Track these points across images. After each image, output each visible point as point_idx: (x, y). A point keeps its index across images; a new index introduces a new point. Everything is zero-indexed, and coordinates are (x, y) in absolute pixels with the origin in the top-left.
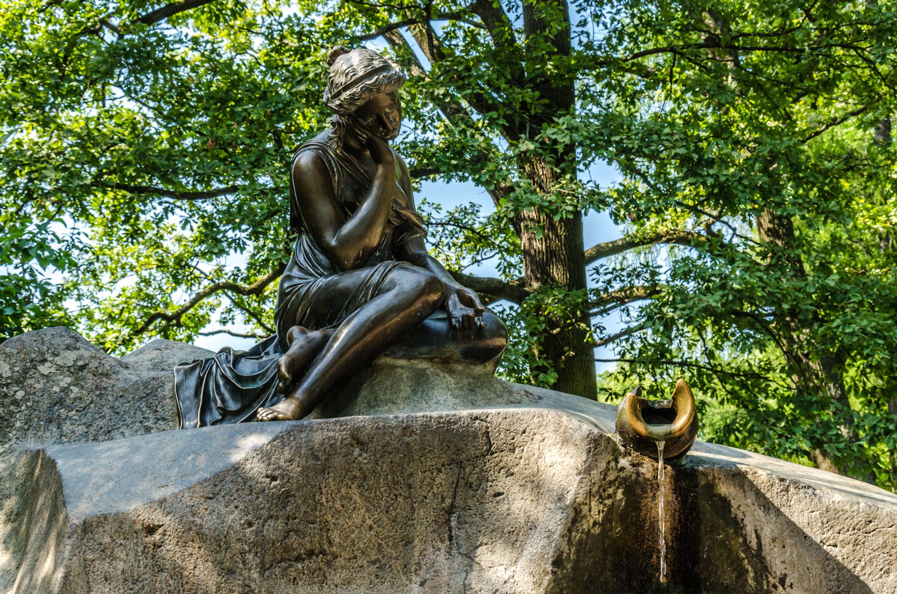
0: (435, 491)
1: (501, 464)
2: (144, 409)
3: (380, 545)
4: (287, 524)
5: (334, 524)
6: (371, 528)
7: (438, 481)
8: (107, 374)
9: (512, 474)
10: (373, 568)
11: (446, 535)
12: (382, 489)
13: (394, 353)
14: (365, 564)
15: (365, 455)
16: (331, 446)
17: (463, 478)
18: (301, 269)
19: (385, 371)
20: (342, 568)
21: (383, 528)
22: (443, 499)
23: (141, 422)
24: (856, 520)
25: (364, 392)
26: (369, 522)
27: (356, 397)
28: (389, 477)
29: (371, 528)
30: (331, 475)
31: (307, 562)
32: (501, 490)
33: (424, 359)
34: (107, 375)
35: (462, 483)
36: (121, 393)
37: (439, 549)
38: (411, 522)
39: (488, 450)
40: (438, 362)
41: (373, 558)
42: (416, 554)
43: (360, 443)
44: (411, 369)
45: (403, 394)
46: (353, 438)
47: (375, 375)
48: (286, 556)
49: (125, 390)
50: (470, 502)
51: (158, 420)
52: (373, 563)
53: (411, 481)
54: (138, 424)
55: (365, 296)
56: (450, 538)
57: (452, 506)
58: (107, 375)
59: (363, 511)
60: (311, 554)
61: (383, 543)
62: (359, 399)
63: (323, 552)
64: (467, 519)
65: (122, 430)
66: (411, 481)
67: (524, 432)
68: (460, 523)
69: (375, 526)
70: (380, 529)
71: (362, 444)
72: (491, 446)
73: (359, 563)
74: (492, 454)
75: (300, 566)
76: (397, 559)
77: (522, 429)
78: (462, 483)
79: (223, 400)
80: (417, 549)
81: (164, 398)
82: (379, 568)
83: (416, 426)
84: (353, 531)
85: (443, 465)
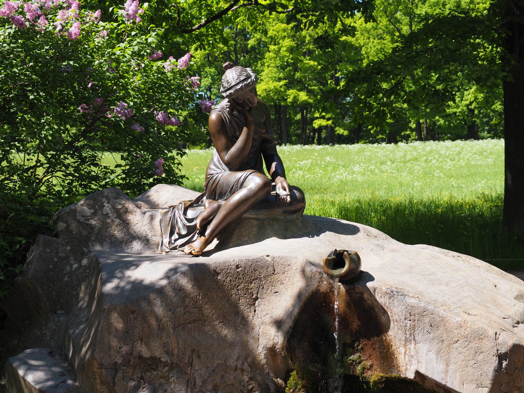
1: (279, 279)
4: (185, 309)
6: (221, 309)
8: (131, 212)
18: (215, 165)
20: (208, 326)
24: (419, 311)
26: (220, 306)
30: (204, 288)
31: (193, 324)
32: (278, 291)
44: (258, 219)
48: (184, 322)
60: (195, 321)
63: (200, 320)
67: (289, 265)
72: (274, 271)
74: (275, 275)
75: (190, 325)
77: (288, 264)
79: (179, 229)
83: (242, 264)
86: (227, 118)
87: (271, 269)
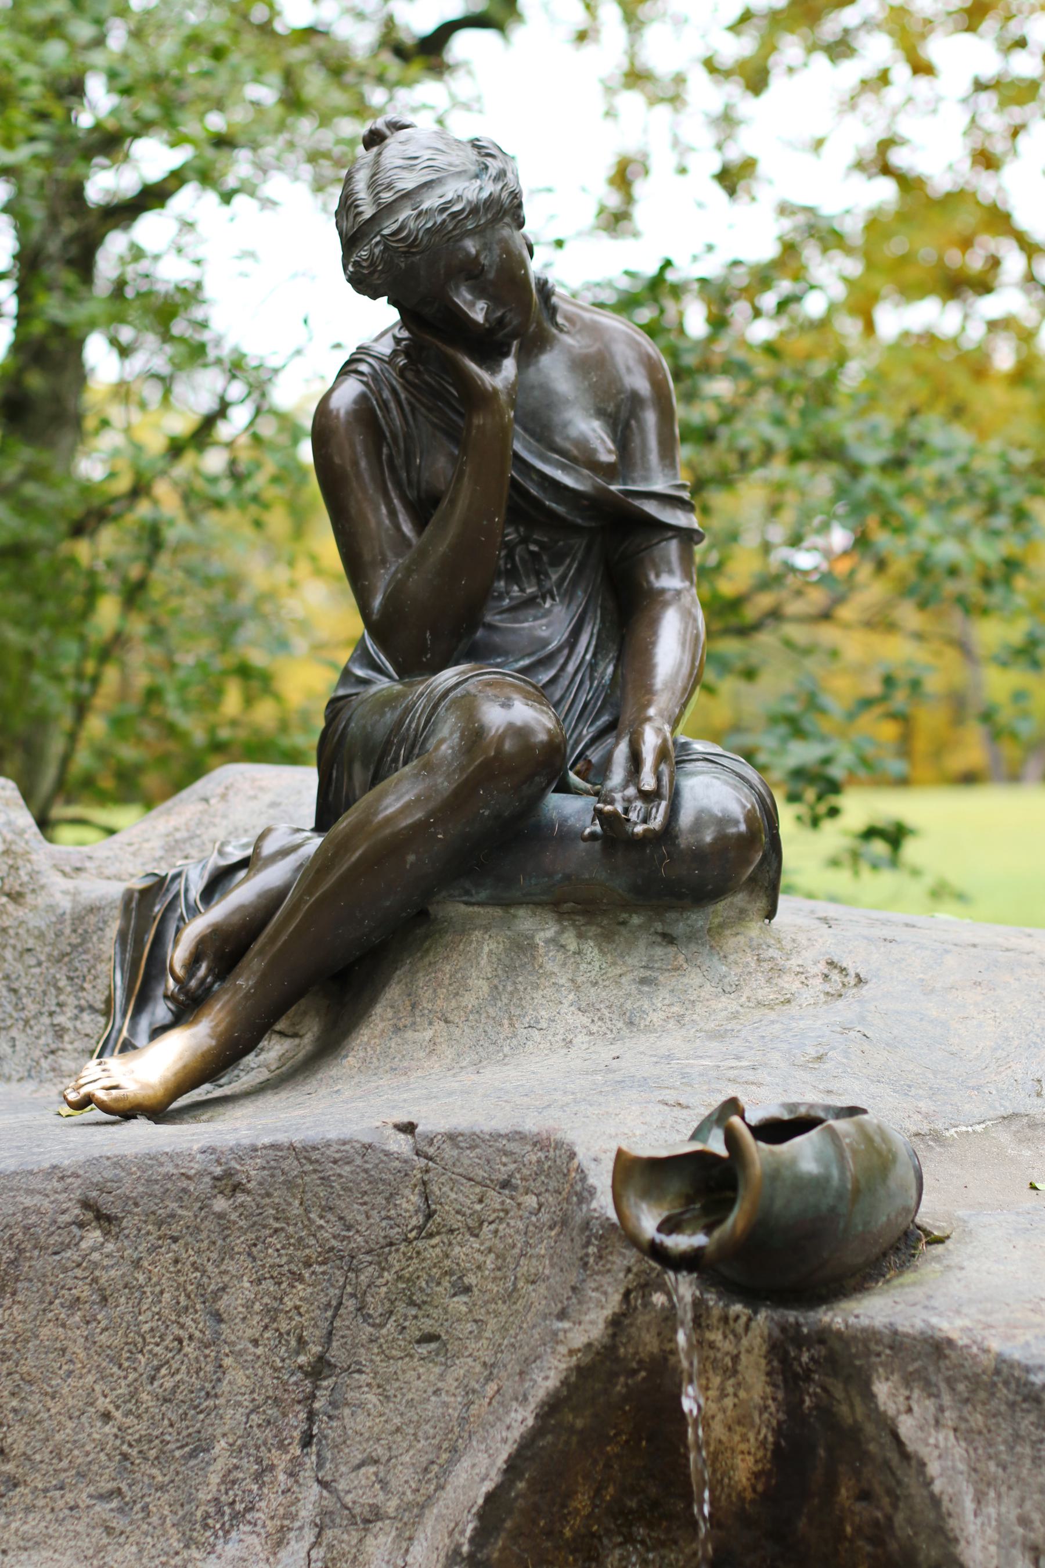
0: (284, 1327)
2: (61, 984)
3: (125, 1457)
5: (15, 1410)
6: (107, 1417)
7: (289, 1304)
9: (467, 1290)
10: (103, 1509)
11: (297, 1434)
12: (146, 1327)
13: (467, 893)
14: (84, 1500)
15: (110, 1247)
16: (27, 1228)
17: (353, 1295)
19: (449, 938)
21: (139, 1417)
22: (300, 1340)
23: (51, 1014)
25: (393, 992)
26: (103, 1404)
27: (373, 1001)
28: (166, 1296)
29: (107, 1417)
33: (538, 904)
34: (16, 897)
35: (350, 1304)
36: (31, 943)
37: (272, 1468)
38: (210, 1403)
39: (420, 1228)
40: (573, 912)
41: (106, 1486)
42: (214, 1479)
43: (104, 1219)
45: (469, 1000)
46: (86, 1204)
47: (427, 944)
49: (41, 936)
50: (363, 1355)
51: (82, 1009)
52: (102, 1497)
53: (221, 1305)
54: (45, 1020)
55: (395, 760)
56: (307, 1440)
57: (321, 1358)
58: (16, 897)
59: (90, 1379)
61: (134, 1452)
62: (378, 1010)
64: (350, 1395)
65: (14, 1033)
66: (221, 1305)
68: (333, 1404)
69: (117, 1414)
70: (130, 1420)
71: (109, 1219)
72: (429, 1216)
73: (70, 1497)
74: (431, 1235)
76: (161, 1488)
78: (350, 1304)
80: (219, 1465)
81: (98, 958)
82: (120, 1510)
83: (251, 1171)
84: (61, 1426)
85: (308, 1264)
86: (392, 405)
87: (410, 1201)
